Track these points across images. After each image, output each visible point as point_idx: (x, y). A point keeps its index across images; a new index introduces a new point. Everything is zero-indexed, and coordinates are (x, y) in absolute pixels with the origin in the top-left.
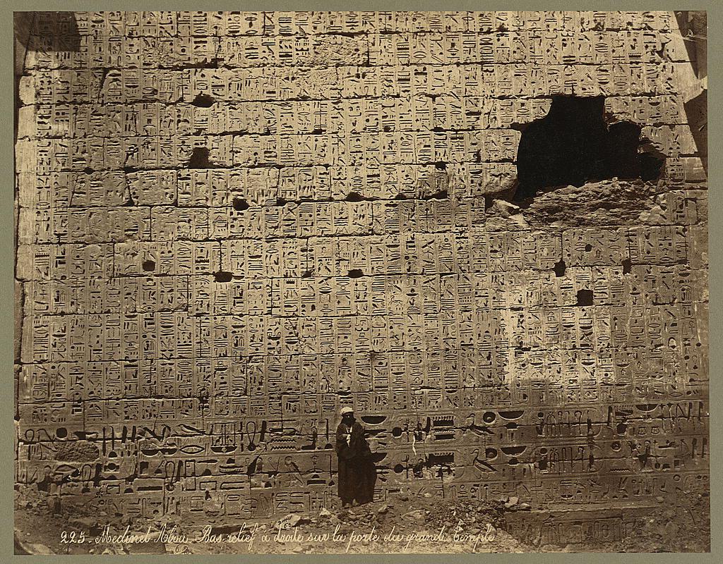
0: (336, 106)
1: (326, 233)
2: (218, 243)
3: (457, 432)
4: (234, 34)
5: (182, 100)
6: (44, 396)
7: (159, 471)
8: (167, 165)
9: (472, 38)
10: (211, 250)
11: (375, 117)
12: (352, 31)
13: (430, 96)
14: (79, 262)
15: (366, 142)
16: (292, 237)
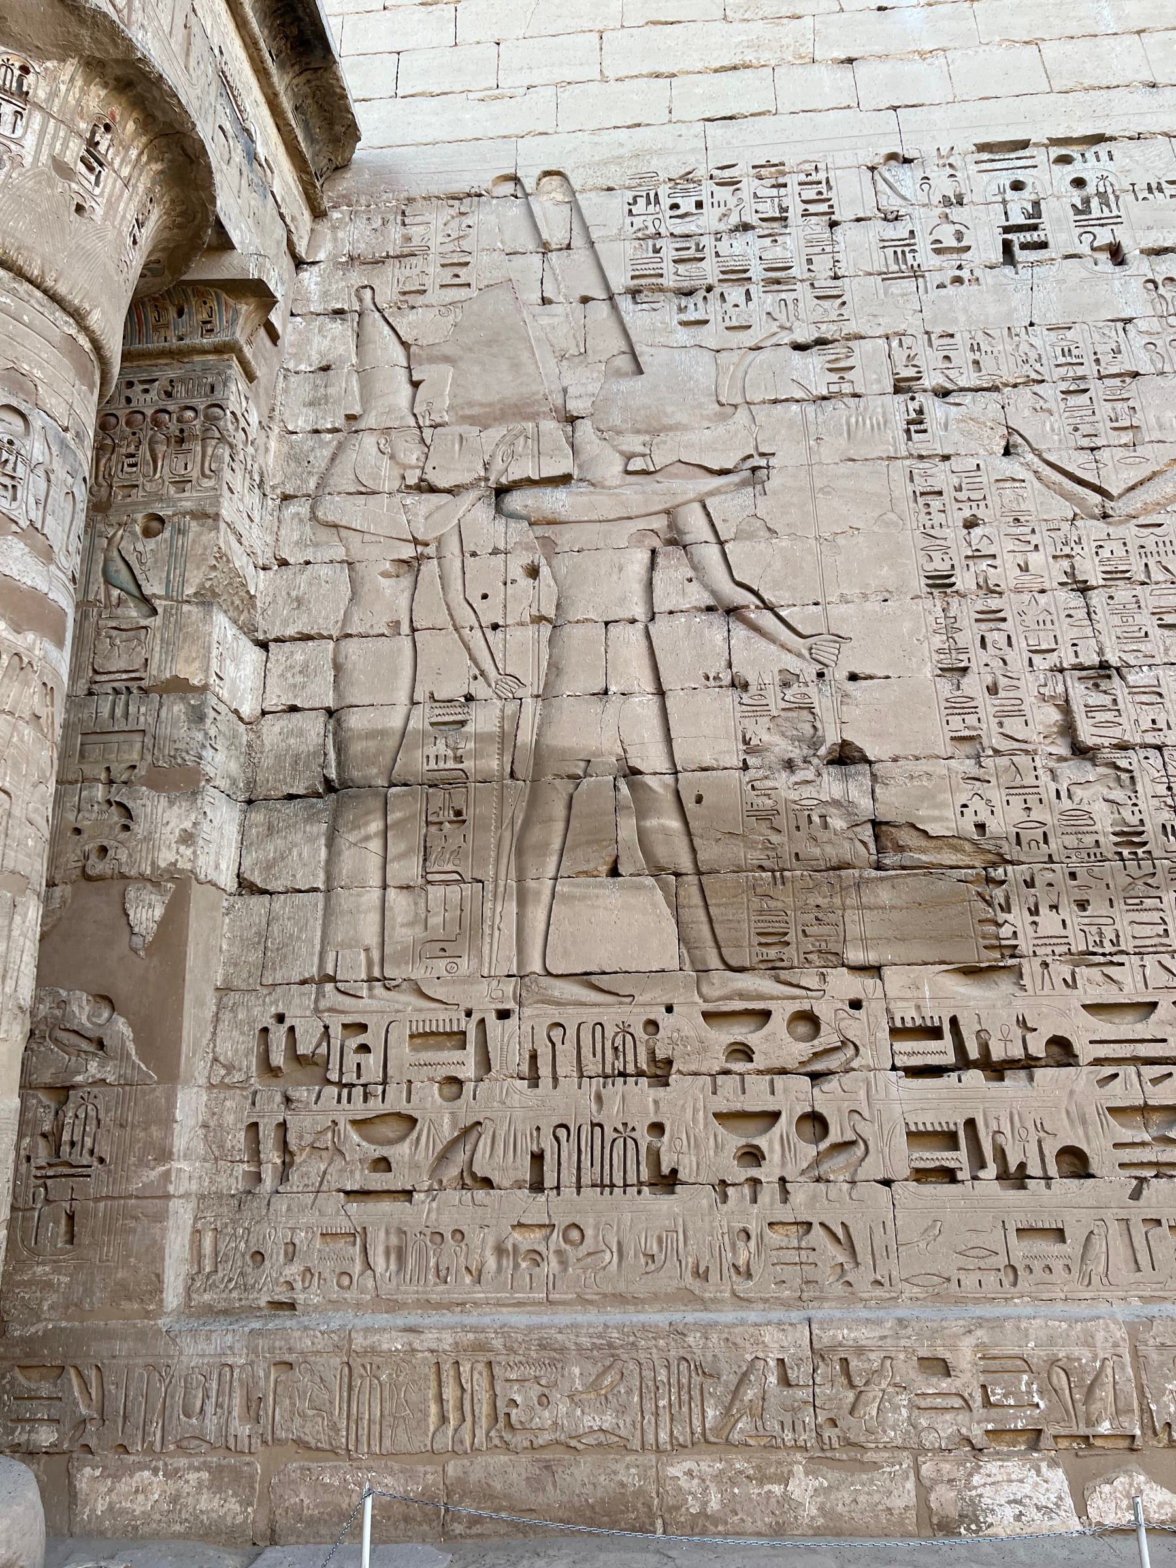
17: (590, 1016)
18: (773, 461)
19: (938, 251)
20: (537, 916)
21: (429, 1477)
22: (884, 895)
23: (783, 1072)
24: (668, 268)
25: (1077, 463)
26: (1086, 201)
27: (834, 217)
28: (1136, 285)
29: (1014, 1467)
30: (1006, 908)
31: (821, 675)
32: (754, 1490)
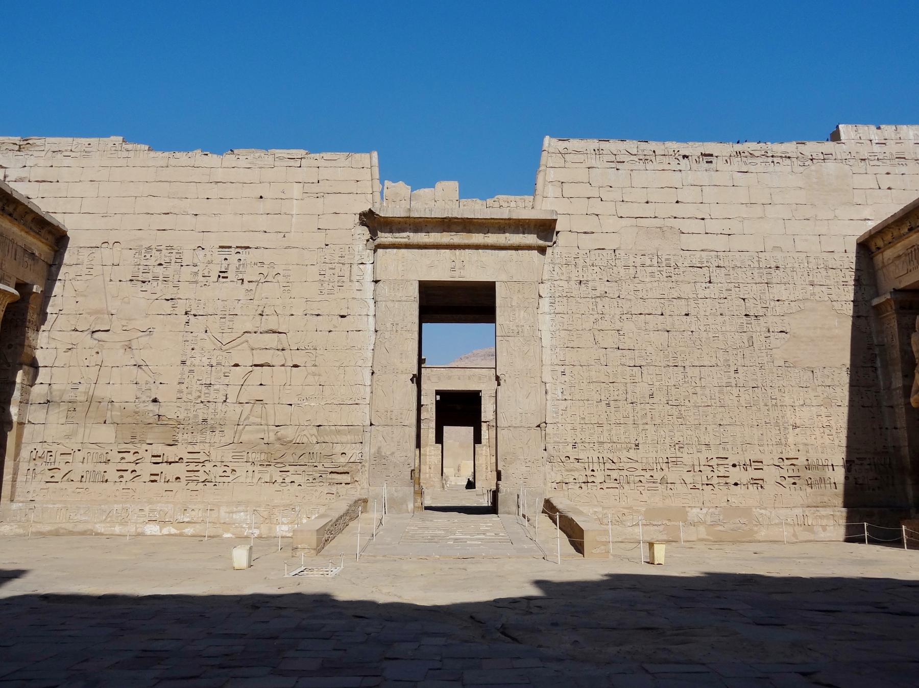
0: (695, 302)
1: (693, 365)
2: (639, 367)
3: (765, 468)
4: (643, 265)
5: (619, 297)
6: (558, 440)
7: (616, 480)
8: (613, 329)
9: (761, 271)
10: (637, 372)
11: (715, 308)
12: (702, 266)
13: (742, 299)
14: (573, 374)
15: (711, 321)
16: (677, 366)
17: (97, 451)
18: (155, 330)
19: (203, 276)
20: (87, 431)
21: (56, 526)
22: (156, 430)
23: (130, 462)
24: (141, 274)
25: (218, 336)
26: (240, 265)
27: (182, 264)
28: (244, 291)
29: (152, 526)
30: (178, 433)
31: (154, 382)
32: (109, 529)
